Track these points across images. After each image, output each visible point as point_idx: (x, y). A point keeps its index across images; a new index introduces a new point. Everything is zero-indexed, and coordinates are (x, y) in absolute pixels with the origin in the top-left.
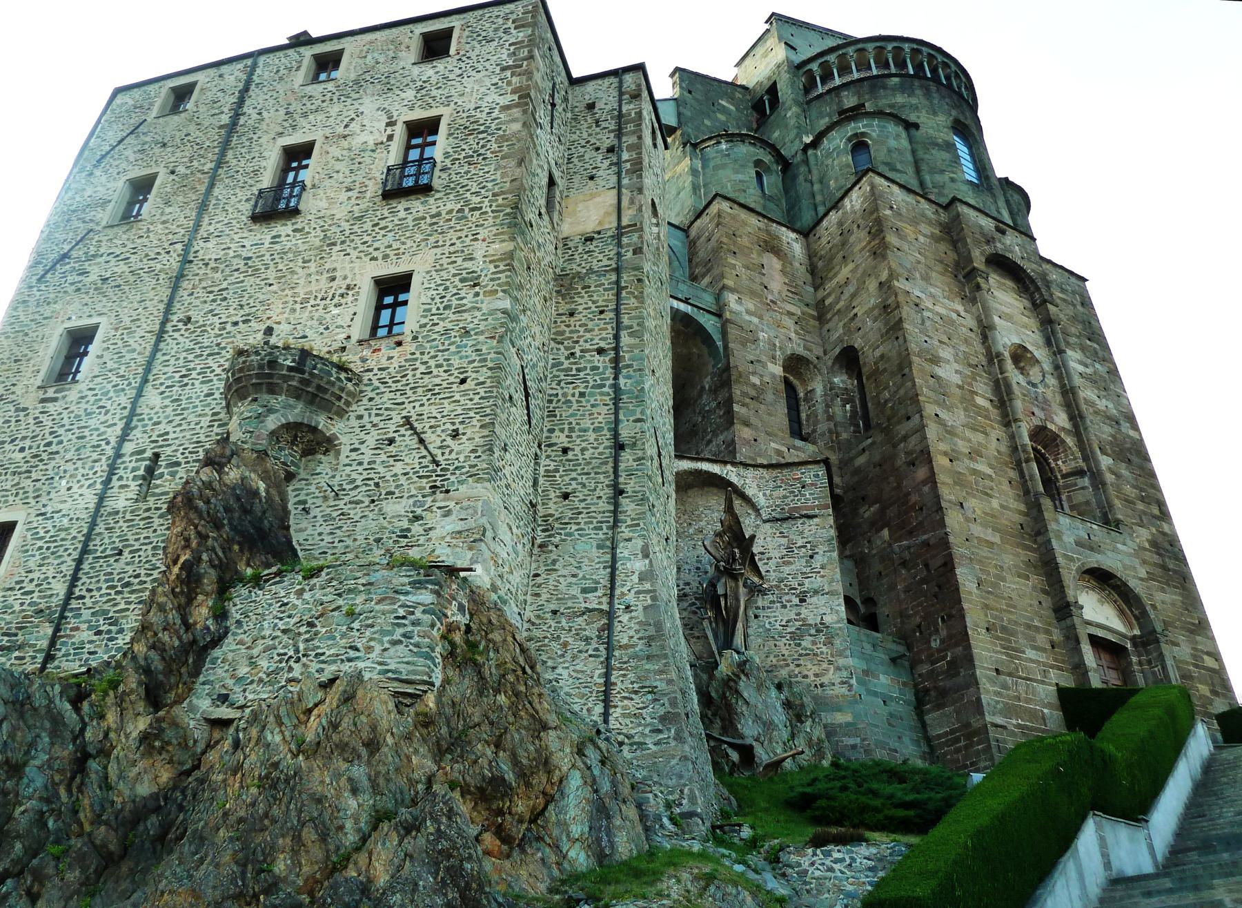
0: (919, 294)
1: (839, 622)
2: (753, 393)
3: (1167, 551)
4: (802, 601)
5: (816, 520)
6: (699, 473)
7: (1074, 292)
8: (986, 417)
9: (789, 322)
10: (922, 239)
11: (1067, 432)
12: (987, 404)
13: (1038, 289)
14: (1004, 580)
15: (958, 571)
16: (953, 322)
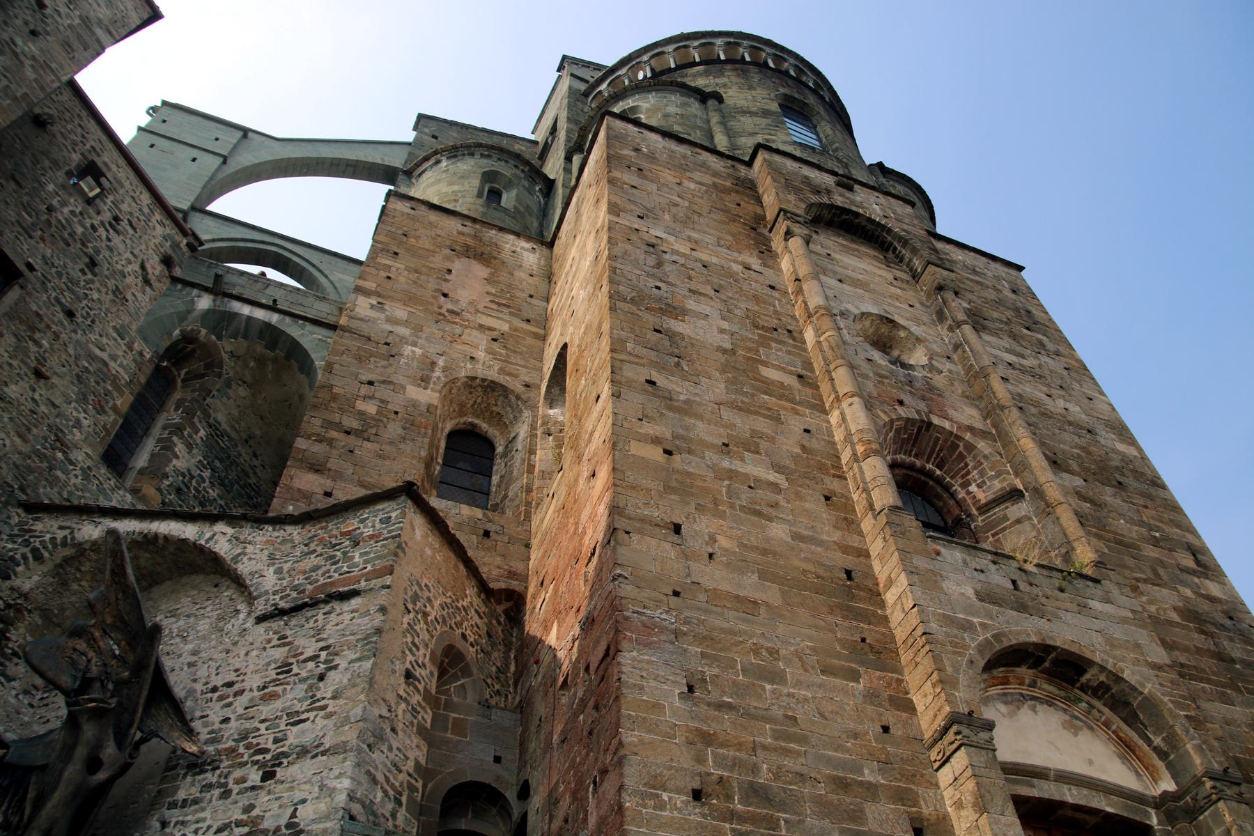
0: (663, 236)
1: (327, 817)
2: (354, 424)
3: (1223, 627)
4: (268, 776)
5: (355, 602)
6: (150, 541)
7: (997, 278)
8: (781, 397)
9: (482, 340)
10: (692, 186)
11: (984, 434)
12: (791, 381)
13: (915, 251)
14: (777, 677)
15: (628, 658)
16: (731, 275)
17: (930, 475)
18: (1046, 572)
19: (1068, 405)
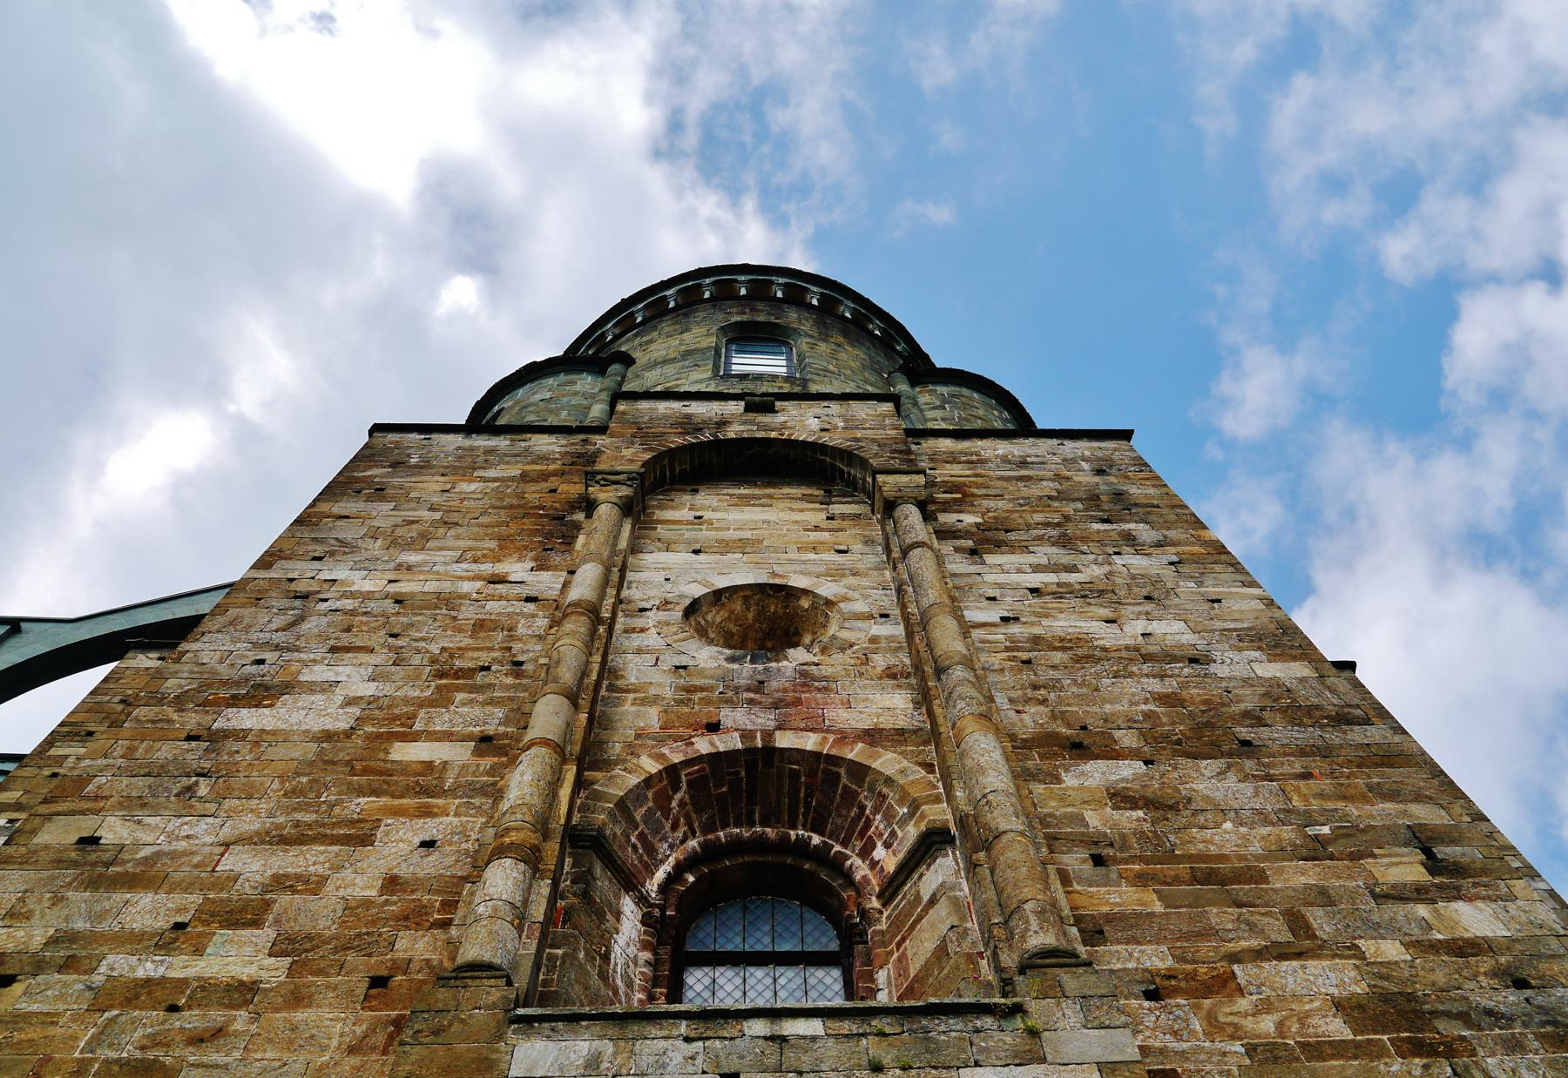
10: (473, 486)
17: (802, 846)
18: (847, 1026)
19: (1157, 627)
